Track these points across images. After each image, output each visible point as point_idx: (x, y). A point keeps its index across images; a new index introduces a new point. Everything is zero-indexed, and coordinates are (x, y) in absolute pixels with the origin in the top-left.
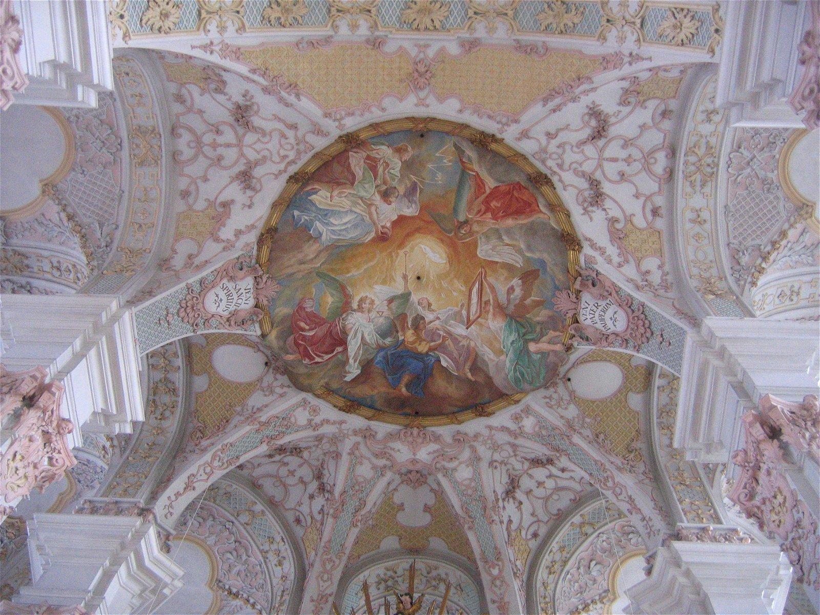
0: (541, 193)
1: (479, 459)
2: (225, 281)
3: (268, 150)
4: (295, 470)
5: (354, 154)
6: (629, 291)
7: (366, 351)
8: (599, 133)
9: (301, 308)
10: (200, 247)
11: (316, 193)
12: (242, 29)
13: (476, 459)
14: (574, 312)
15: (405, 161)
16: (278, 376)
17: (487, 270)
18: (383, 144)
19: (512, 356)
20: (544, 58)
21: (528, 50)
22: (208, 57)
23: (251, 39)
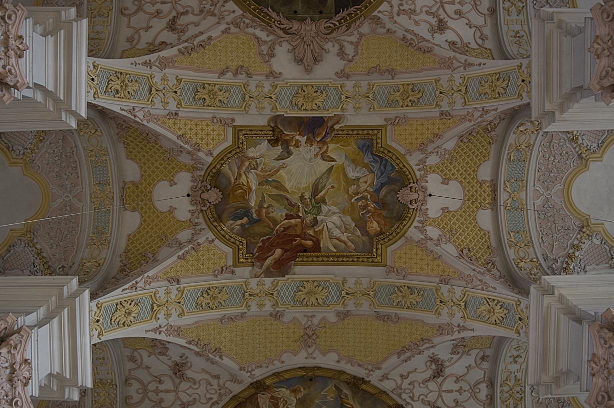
3: (197, 394)
5: (262, 396)
8: (438, 373)
15: (299, 398)
18: (284, 387)
20: (397, 324)
21: (386, 318)
23: (188, 320)
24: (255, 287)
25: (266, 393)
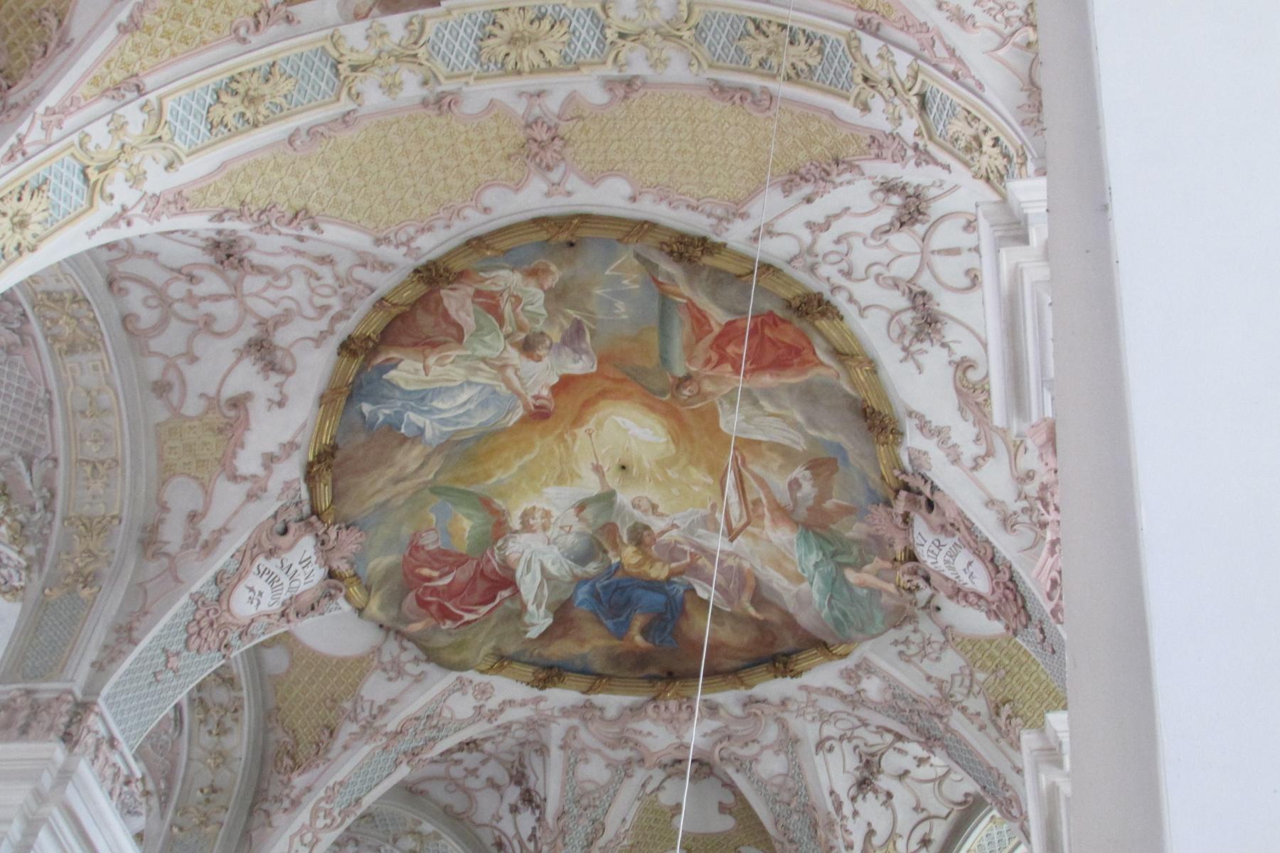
1: (796, 741)
2: (261, 560)
5: (451, 293)
6: (986, 534)
7: (553, 589)
9: (415, 547)
11: (394, 367)
13: (789, 743)
17: (745, 454)
18: (503, 268)
19: (821, 585)
23: (194, 169)
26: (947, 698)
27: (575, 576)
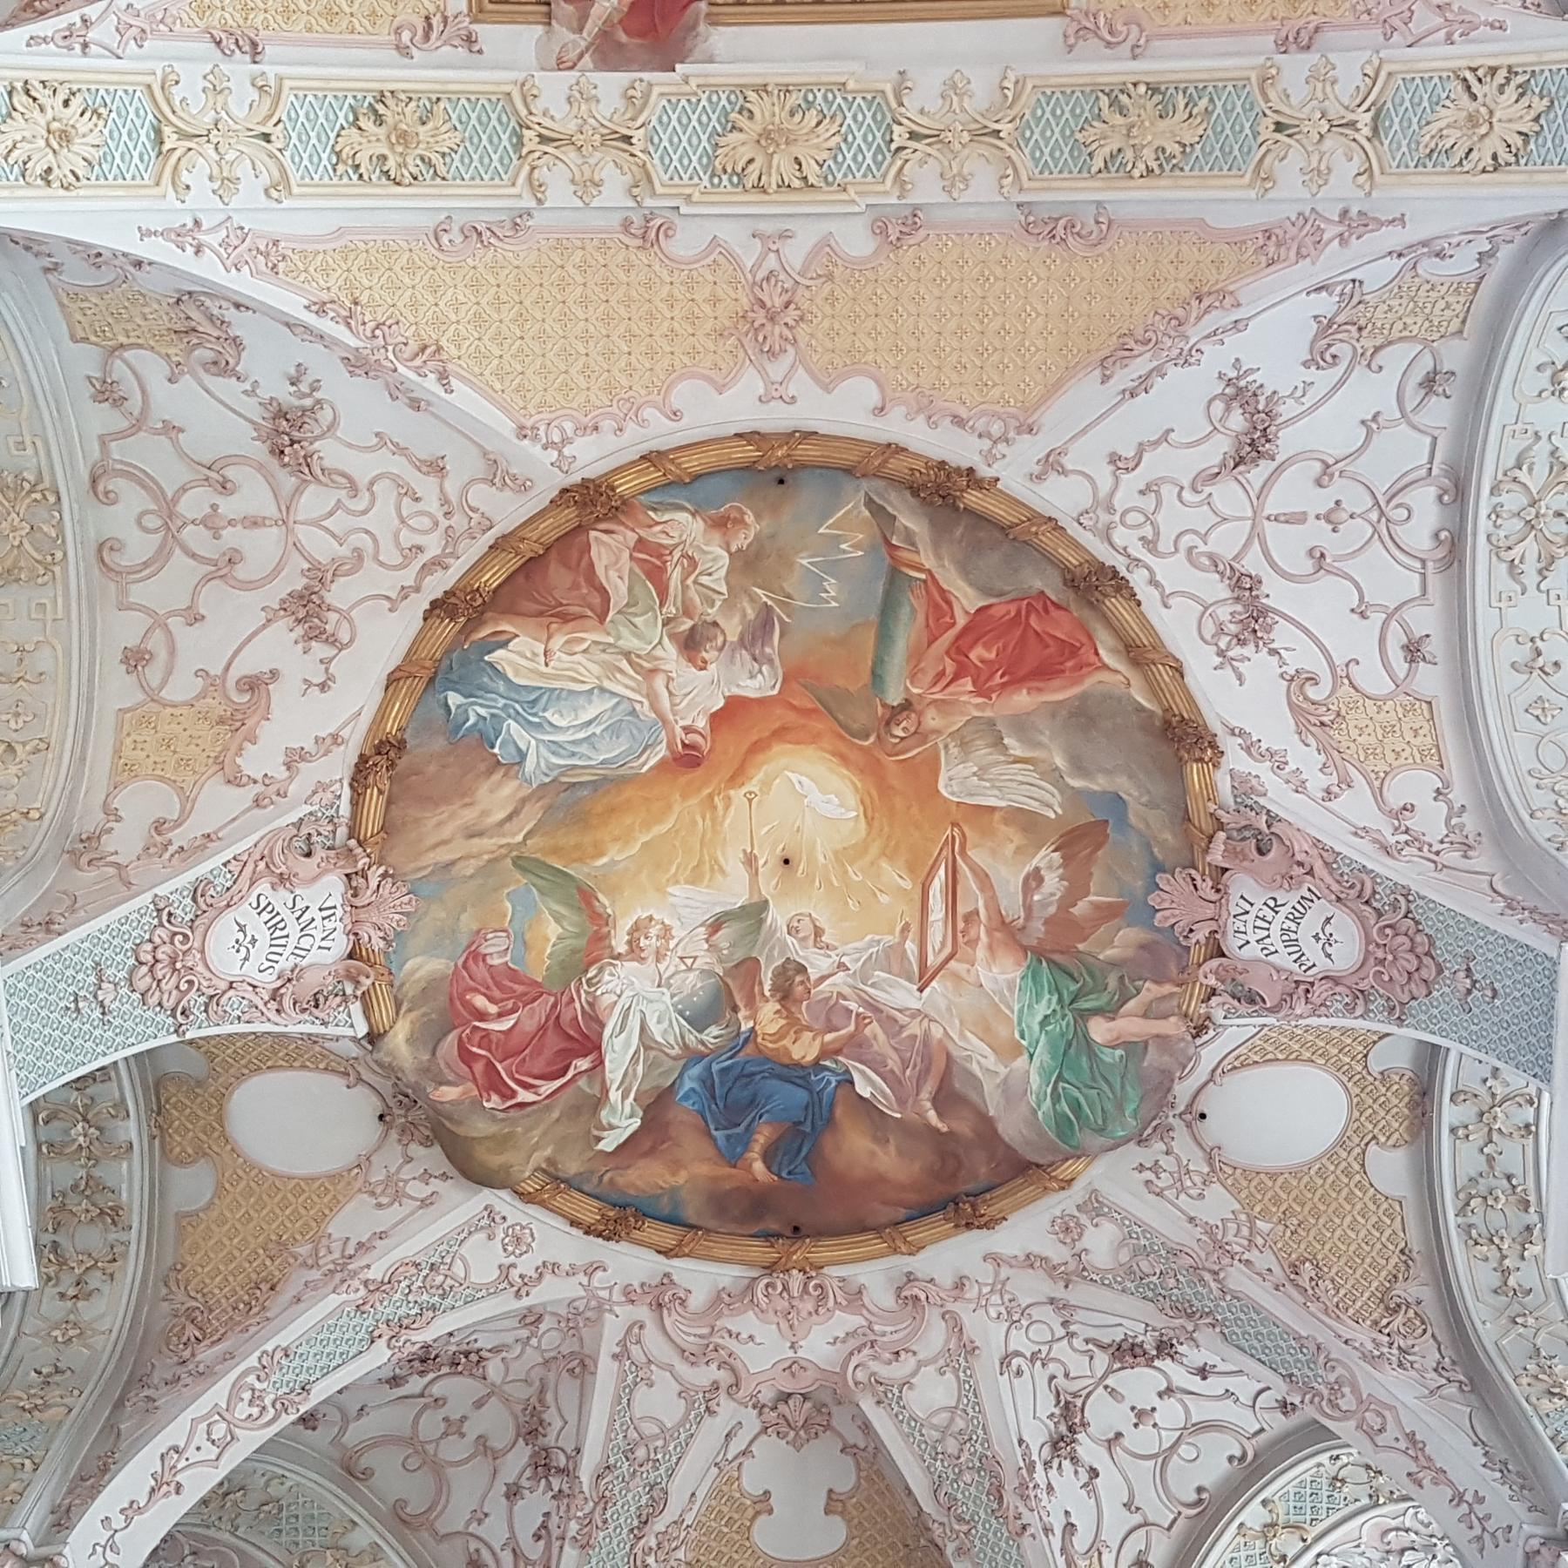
0: (1104, 616)
1: (971, 1350)
2: (263, 887)
3: (367, 532)
4: (464, 1419)
5: (604, 537)
7: (650, 1067)
9: (475, 956)
10: (188, 803)
11: (504, 645)
12: (279, 186)
14: (1213, 926)
15: (739, 550)
16: (416, 1149)
17: (966, 829)
18: (682, 508)
19: (1047, 1058)
20: (1101, 249)
22: (184, 261)
24: (559, 110)
25: (622, 528)
26: (1220, 1246)
27: (685, 1046)
